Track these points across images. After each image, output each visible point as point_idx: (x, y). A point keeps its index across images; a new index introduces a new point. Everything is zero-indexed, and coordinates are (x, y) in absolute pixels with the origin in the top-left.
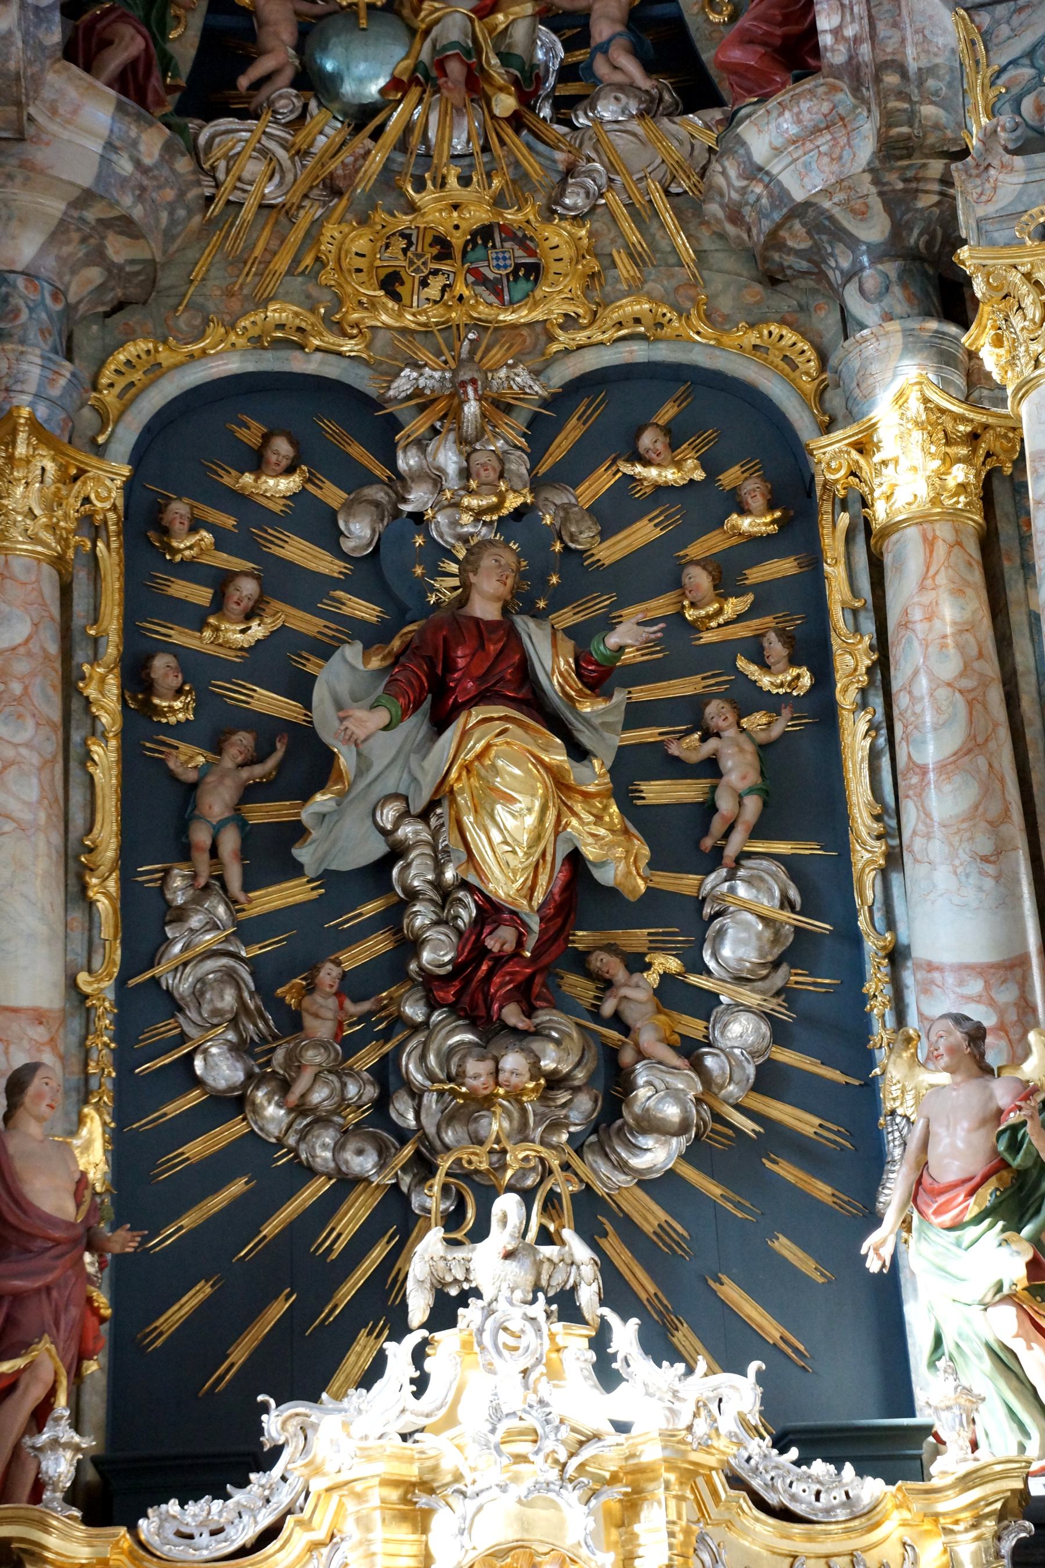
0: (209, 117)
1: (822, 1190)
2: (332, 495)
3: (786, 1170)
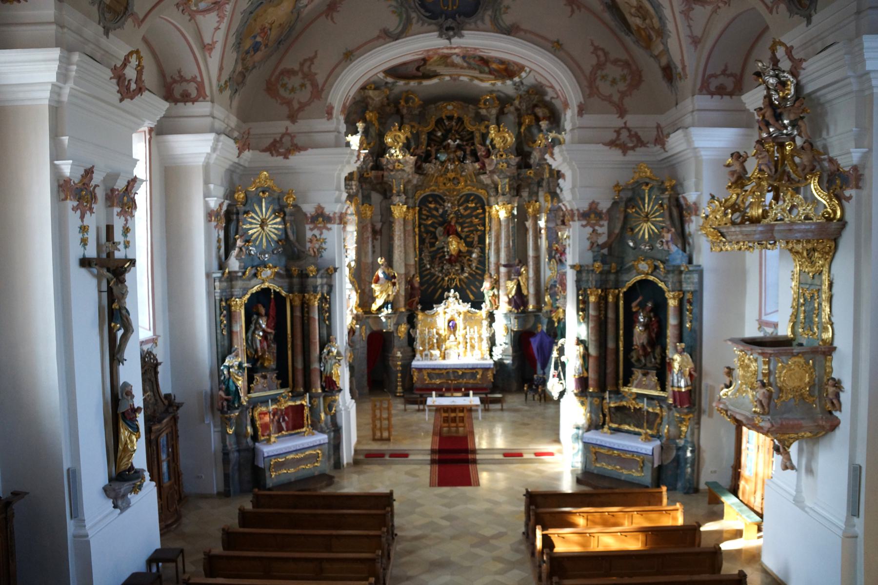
0: (426, 163)
1: (481, 278)
2: (438, 206)
3: (478, 277)
